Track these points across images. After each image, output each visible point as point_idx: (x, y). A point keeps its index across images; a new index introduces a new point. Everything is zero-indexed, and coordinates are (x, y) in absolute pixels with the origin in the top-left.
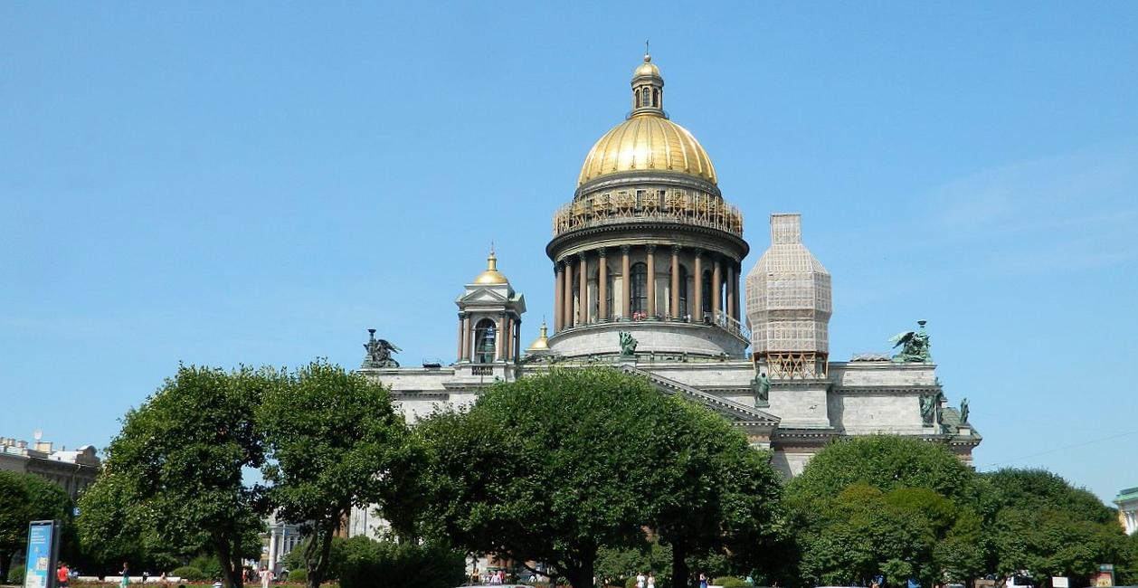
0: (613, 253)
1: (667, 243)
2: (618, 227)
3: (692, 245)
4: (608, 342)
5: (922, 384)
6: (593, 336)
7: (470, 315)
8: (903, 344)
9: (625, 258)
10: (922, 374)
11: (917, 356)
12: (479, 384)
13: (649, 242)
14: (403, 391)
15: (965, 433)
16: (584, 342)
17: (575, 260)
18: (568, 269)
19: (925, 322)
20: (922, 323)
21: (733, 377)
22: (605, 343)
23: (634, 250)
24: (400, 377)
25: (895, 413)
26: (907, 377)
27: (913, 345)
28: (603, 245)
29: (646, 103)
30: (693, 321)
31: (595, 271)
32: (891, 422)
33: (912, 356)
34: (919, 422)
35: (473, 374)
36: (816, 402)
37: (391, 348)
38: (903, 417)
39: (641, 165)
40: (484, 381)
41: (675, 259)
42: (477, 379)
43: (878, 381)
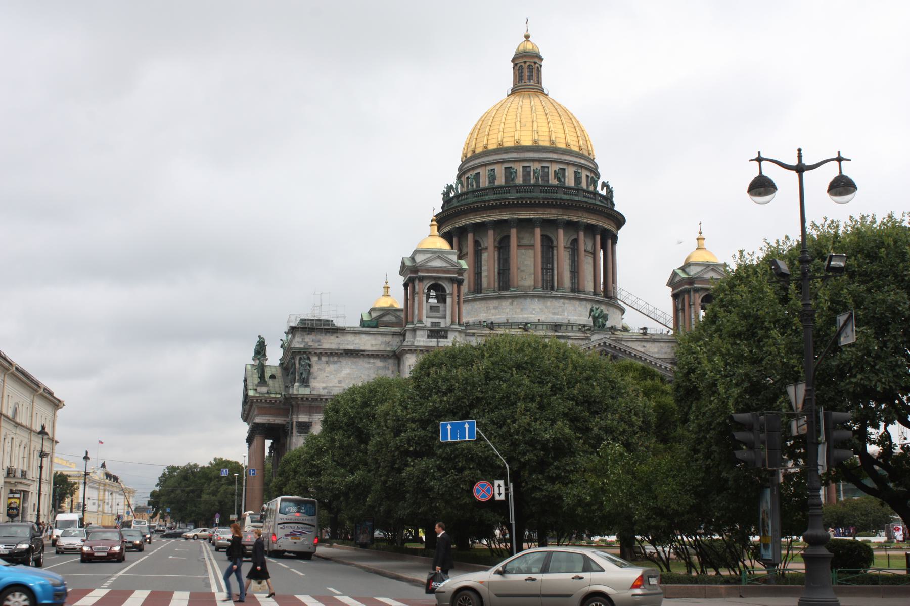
0: (526, 225)
1: (575, 219)
2: (533, 201)
4: (522, 310)
6: (506, 304)
7: (421, 279)
9: (538, 231)
13: (560, 217)
14: (345, 350)
16: (496, 308)
17: (480, 228)
21: (656, 350)
28: (515, 217)
30: (595, 294)
31: (499, 238)
35: (429, 337)
41: (582, 234)
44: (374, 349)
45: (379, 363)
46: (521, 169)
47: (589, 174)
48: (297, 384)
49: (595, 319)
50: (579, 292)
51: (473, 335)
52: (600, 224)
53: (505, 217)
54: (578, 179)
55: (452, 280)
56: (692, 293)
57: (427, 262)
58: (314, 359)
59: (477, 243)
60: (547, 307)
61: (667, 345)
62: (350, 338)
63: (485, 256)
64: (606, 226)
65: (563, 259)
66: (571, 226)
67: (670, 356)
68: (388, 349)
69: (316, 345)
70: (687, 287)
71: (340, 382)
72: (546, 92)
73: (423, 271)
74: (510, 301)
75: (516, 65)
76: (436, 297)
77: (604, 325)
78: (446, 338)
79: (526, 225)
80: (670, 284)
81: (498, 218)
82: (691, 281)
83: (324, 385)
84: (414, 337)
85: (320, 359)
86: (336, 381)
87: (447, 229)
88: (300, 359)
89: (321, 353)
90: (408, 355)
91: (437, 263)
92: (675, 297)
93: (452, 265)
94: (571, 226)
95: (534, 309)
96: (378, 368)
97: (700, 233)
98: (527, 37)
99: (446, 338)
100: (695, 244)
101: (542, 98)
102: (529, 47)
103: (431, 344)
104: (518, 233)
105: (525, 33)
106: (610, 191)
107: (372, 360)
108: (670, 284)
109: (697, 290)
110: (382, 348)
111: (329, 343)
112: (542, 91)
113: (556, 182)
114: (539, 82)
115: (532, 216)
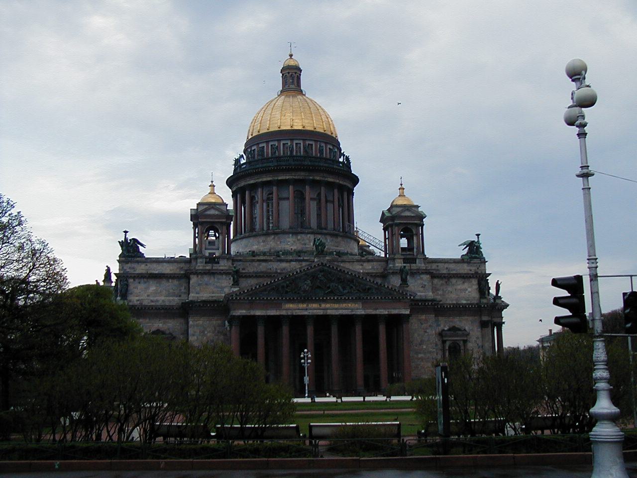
1: (318, 178)
5: (480, 272)
8: (468, 248)
9: (291, 187)
10: (479, 266)
11: (477, 255)
12: (209, 270)
13: (307, 178)
14: (151, 274)
15: (498, 301)
16: (264, 241)
17: (253, 187)
19: (479, 235)
20: (478, 235)
21: (370, 267)
22: (279, 243)
23: (296, 182)
24: (147, 264)
26: (471, 268)
27: (474, 248)
32: (462, 294)
33: (473, 256)
35: (206, 263)
36: (426, 283)
37: (142, 245)
38: (469, 292)
39: (298, 126)
40: (214, 268)
41: (323, 189)
42: (208, 267)
43: (454, 270)
44: (172, 272)
45: (176, 282)
47: (332, 148)
49: (317, 247)
50: (322, 229)
52: (338, 181)
53: (269, 179)
56: (394, 226)
57: (204, 212)
59: (252, 198)
60: (298, 240)
61: (379, 263)
62: (155, 265)
63: (258, 206)
64: (341, 182)
65: (312, 207)
67: (380, 271)
68: (182, 272)
69: (132, 271)
70: (390, 223)
71: (148, 296)
72: (304, 93)
75: (283, 75)
76: (215, 235)
77: (323, 251)
78: (218, 263)
81: (265, 179)
82: (393, 218)
83: (138, 298)
85: (134, 280)
86: (146, 295)
87: (234, 189)
88: (121, 281)
89: (135, 277)
90: (192, 276)
91: (212, 212)
92: (385, 229)
93: (222, 213)
94: (315, 184)
95: (289, 242)
97: (401, 185)
98: (291, 56)
99: (218, 263)
100: (398, 193)
101: (300, 97)
102: (292, 63)
103: (207, 268)
104: (278, 190)
105: (289, 53)
107: (170, 281)
109: (397, 225)
110: (178, 272)
112: (301, 91)
114: (299, 84)
115: (287, 178)
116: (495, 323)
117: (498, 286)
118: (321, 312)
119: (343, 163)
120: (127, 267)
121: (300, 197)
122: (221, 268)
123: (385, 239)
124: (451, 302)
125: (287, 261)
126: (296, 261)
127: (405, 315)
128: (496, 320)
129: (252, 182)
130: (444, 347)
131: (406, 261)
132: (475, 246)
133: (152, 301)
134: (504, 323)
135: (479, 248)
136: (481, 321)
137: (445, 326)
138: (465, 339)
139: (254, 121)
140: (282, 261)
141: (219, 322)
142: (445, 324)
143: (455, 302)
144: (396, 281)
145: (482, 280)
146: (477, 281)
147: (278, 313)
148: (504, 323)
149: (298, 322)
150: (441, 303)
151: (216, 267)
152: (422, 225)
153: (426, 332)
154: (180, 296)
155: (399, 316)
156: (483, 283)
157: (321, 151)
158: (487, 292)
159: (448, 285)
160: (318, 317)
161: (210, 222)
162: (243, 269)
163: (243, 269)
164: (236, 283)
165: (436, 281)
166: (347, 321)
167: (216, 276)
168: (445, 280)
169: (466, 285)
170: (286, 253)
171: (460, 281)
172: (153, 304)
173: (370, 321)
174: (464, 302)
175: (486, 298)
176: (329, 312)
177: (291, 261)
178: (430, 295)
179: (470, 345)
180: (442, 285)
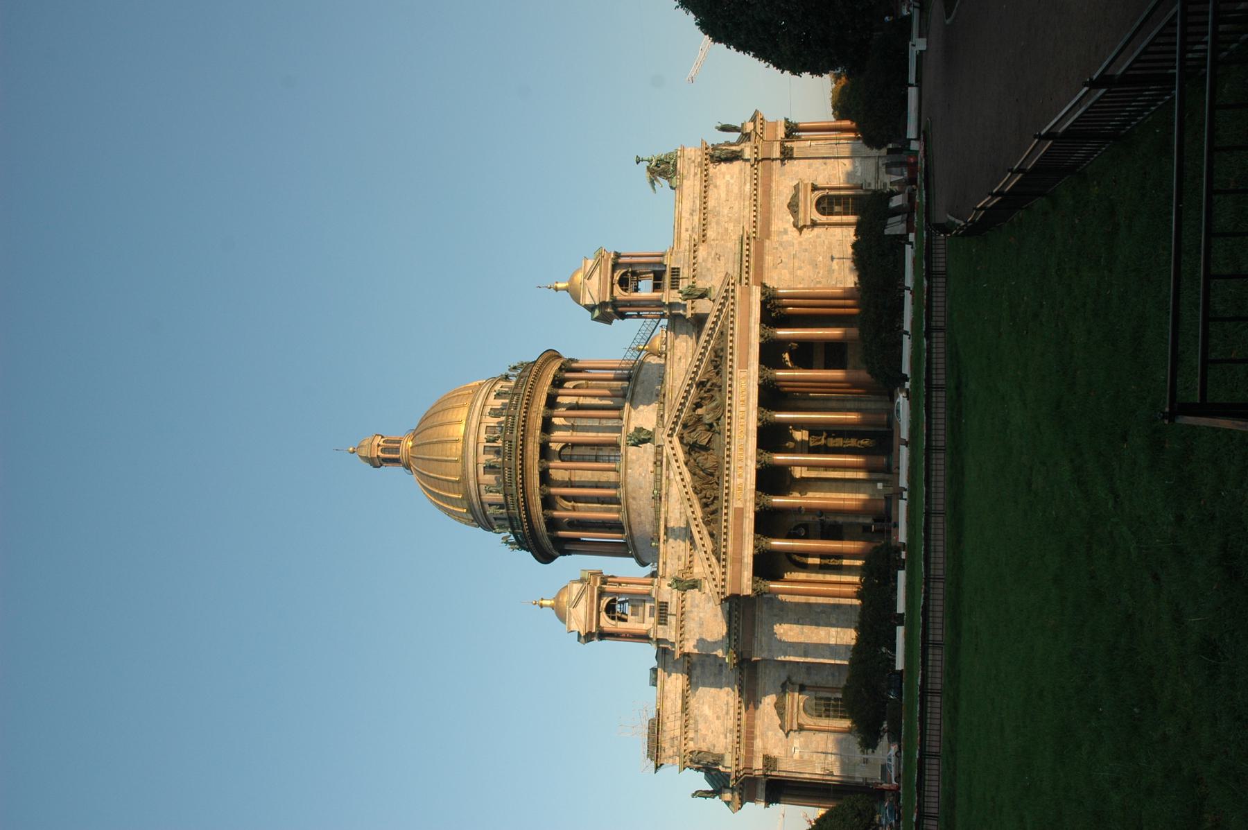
1: (540, 422)
3: (544, 398)
13: (538, 440)
15: (749, 127)
16: (640, 515)
18: (562, 533)
25: (728, 184)
29: (397, 450)
32: (736, 190)
34: (737, 165)
38: (732, 177)
46: (487, 477)
48: (720, 767)
51: (664, 563)
52: (546, 389)
53: (539, 502)
54: (495, 413)
55: (601, 594)
58: (691, 746)
66: (547, 426)
71: (718, 718)
73: (591, 627)
74: (630, 500)
79: (545, 477)
80: (610, 322)
81: (540, 508)
83: (722, 737)
84: (665, 641)
85: (692, 739)
87: (556, 553)
92: (623, 316)
94: (547, 426)
96: (703, 673)
106: (515, 368)
108: (610, 322)
111: (672, 727)
113: (499, 443)
116: (787, 136)
117: (725, 129)
118: (753, 441)
119: (520, 377)
120: (669, 752)
121: (571, 451)
122: (675, 599)
123: (639, 316)
124: (747, 210)
125: (669, 485)
126: (668, 469)
127: (762, 294)
128: (781, 133)
129: (543, 527)
130: (823, 224)
131: (674, 285)
132: (656, 165)
133: (727, 713)
134: (786, 120)
135: (660, 161)
136: (782, 160)
137: (788, 222)
138: (809, 188)
139: (450, 513)
140: (667, 494)
141: (765, 607)
142: (782, 221)
143: (747, 203)
144: (703, 306)
145: (712, 156)
146: (711, 165)
147: (752, 516)
148: (786, 120)
149: (771, 479)
150: (746, 228)
151: (672, 609)
152: (618, 256)
153: (795, 256)
154: (721, 665)
155: (763, 304)
156: (717, 153)
157: (495, 413)
158: (734, 148)
159: (719, 213)
160: (759, 446)
161: (599, 613)
162: (679, 559)
163: (679, 559)
164: (695, 585)
165: (711, 234)
166: (771, 396)
167: (687, 608)
168: (709, 217)
169: (720, 182)
170: (657, 481)
171: (712, 193)
172: (731, 712)
173: (770, 354)
174: (748, 186)
175: (742, 151)
176: (753, 425)
177: (668, 478)
178: (732, 245)
179: (821, 182)
180: (718, 223)
